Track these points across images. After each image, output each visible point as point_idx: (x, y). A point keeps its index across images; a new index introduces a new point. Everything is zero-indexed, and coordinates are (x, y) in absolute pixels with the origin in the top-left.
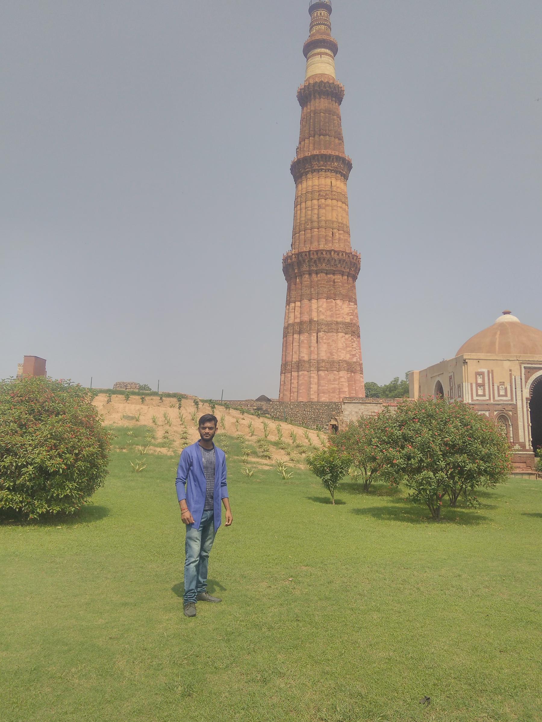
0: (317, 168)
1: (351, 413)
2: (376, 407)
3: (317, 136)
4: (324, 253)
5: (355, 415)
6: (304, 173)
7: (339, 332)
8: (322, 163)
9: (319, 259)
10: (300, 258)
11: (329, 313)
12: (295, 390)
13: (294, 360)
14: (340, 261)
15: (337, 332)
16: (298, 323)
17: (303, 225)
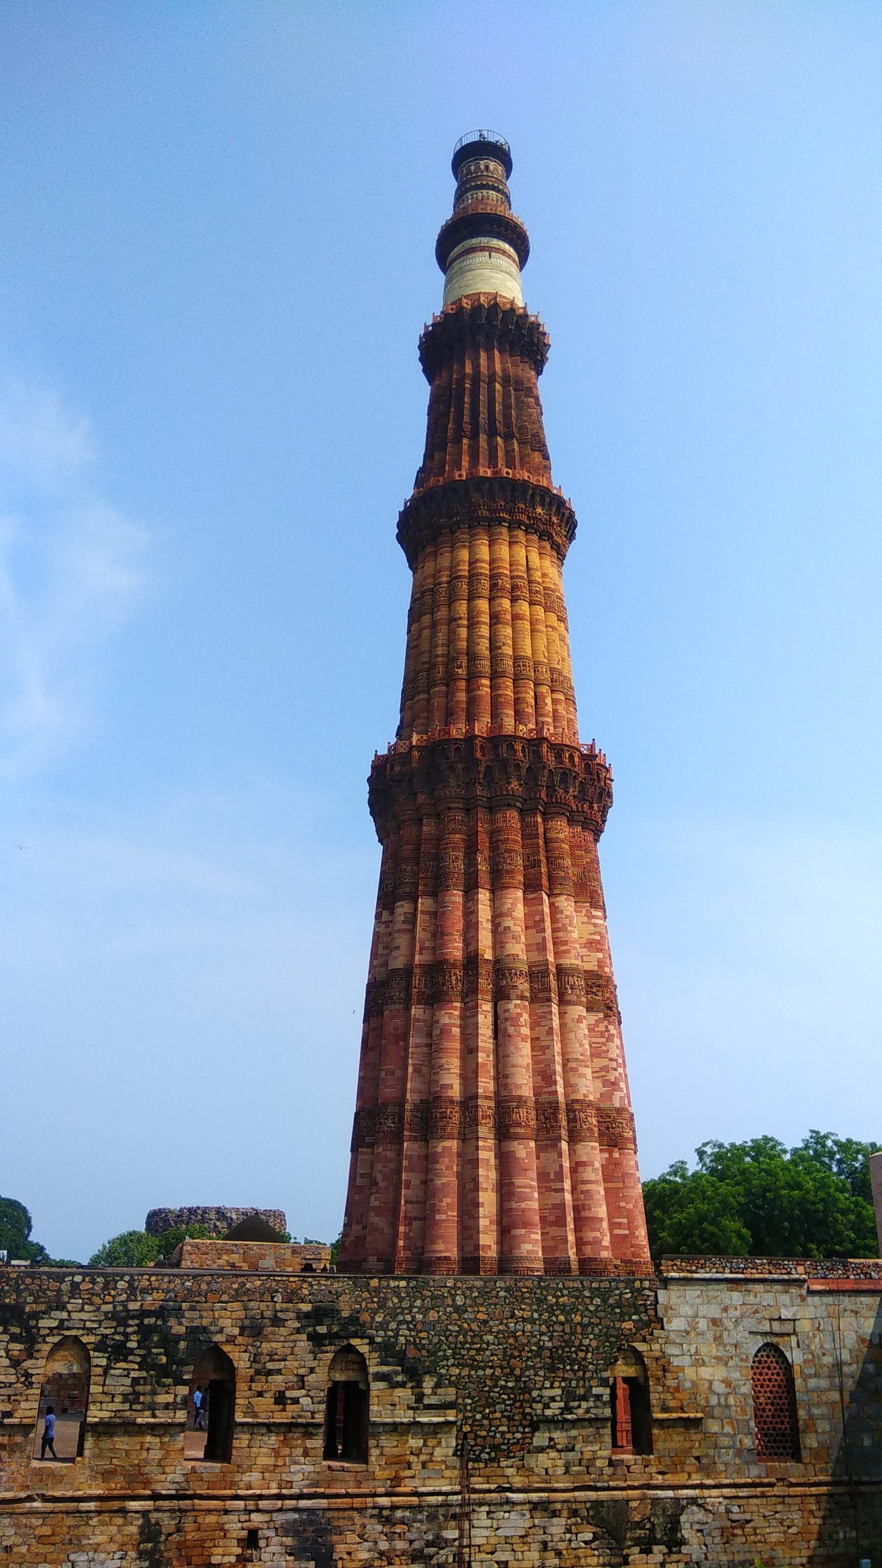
0: (485, 513)
2: (785, 1299)
5: (710, 1335)
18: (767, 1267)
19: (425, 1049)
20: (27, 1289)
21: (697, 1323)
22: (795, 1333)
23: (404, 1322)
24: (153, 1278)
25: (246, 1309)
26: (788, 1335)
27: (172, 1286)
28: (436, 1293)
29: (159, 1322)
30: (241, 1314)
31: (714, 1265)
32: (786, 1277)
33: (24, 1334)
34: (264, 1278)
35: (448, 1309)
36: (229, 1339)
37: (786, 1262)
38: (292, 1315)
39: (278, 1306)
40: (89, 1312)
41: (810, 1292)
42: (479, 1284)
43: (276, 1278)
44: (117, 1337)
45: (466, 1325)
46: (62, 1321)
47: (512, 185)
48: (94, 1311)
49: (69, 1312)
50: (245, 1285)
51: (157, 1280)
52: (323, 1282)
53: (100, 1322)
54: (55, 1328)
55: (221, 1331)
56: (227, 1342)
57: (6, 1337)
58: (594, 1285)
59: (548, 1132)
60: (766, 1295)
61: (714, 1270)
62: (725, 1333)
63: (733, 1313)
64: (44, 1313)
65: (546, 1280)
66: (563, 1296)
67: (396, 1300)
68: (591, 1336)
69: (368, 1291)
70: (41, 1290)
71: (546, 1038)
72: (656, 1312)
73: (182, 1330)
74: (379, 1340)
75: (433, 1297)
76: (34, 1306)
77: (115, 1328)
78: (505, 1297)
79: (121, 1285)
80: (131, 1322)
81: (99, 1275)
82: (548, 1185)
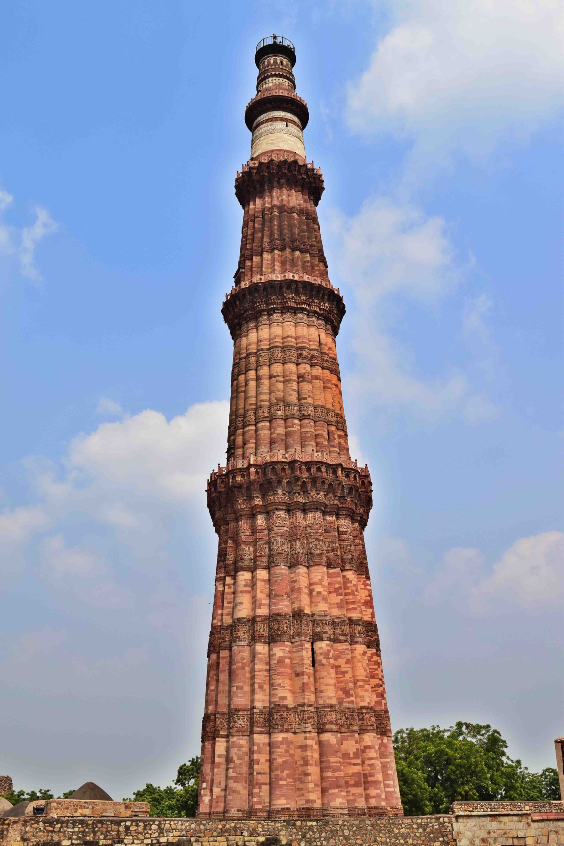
0: (293, 305)
2: (520, 825)
3: (288, 250)
4: (323, 469)
6: (264, 310)
7: (357, 643)
8: (303, 297)
9: (314, 481)
10: (270, 475)
11: (335, 599)
12: (264, 779)
13: (259, 705)
14: (351, 489)
15: (353, 642)
16: (264, 618)
17: (266, 410)
18: (509, 807)
19: (266, 673)
20: (99, 831)
24: (172, 823)
25: (227, 840)
27: (183, 827)
28: (333, 828)
31: (482, 806)
32: (520, 812)
34: (236, 822)
35: (340, 838)
37: (519, 804)
39: (246, 838)
40: (137, 844)
41: (534, 821)
42: (357, 822)
43: (243, 821)
47: (295, 71)
48: (140, 844)
50: (225, 825)
51: (174, 824)
52: (270, 824)
58: (419, 821)
59: (348, 727)
61: (482, 810)
63: (493, 835)
65: (392, 819)
66: (402, 828)
67: (311, 833)
69: (295, 828)
70: (107, 831)
71: (346, 666)
72: (453, 836)
75: (331, 831)
76: (105, 841)
78: (371, 830)
79: (154, 827)
81: (140, 821)
82: (349, 761)
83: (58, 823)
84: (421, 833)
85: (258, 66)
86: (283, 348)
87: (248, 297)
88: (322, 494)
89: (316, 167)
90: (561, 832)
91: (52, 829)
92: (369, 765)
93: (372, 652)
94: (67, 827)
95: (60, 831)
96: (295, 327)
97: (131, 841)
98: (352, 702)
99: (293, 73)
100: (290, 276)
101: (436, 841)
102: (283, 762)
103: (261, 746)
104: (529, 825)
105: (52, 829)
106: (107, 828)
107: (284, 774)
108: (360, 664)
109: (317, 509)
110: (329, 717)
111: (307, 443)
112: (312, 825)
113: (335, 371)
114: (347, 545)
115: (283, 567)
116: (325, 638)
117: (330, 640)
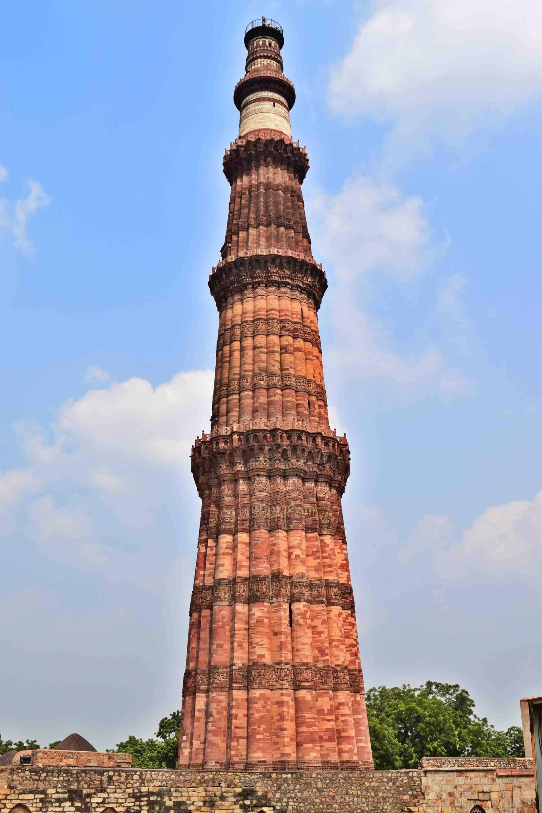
0: (277, 279)
1: (439, 797)
2: (485, 780)
3: (273, 226)
4: (304, 438)
5: (448, 802)
6: (249, 284)
7: (333, 604)
8: (287, 272)
9: (294, 448)
10: (252, 443)
11: (313, 562)
12: (242, 733)
13: (238, 662)
14: (330, 457)
15: (329, 603)
16: (245, 580)
17: (249, 380)
18: (476, 763)
20: (83, 780)
21: (441, 795)
22: (490, 800)
23: (291, 797)
24: (153, 773)
25: (206, 791)
26: (487, 800)
27: (164, 778)
28: (307, 781)
29: (159, 799)
30: (203, 794)
31: (450, 762)
32: (486, 768)
33: (83, 807)
34: (214, 773)
35: (314, 790)
36: (198, 808)
37: (485, 760)
38: (231, 794)
39: (224, 789)
41: (499, 777)
42: (330, 775)
44: (136, 808)
45: (323, 799)
46: (104, 799)
48: (122, 793)
49: (108, 793)
50: (204, 776)
51: (155, 774)
53: (126, 799)
54: (101, 803)
55: (193, 804)
56: (197, 810)
57: (73, 809)
58: (389, 775)
59: (323, 685)
60: (475, 779)
61: (450, 765)
62: (456, 800)
63: (459, 789)
64: (95, 794)
65: (364, 773)
66: (373, 781)
67: (286, 785)
68: (388, 804)
69: (271, 780)
72: (421, 789)
73: (171, 803)
74: (278, 808)
75: (305, 784)
76: (88, 790)
77: (134, 802)
79: (136, 777)
80: (143, 799)
81: (123, 771)
82: (323, 717)
83: (43, 772)
84: (391, 787)
85: (247, 47)
86: (267, 320)
87: (234, 270)
88: (302, 461)
89: (301, 146)
90: (524, 787)
91: (38, 778)
92: (342, 721)
93: (347, 614)
94: (52, 776)
95: (45, 780)
96: (279, 300)
97: (114, 790)
98: (327, 661)
99: (281, 55)
100: (274, 251)
101: (405, 795)
102: (260, 717)
103: (240, 701)
104: (494, 780)
105: (38, 778)
106: (90, 778)
107: (261, 729)
108: (335, 625)
109: (297, 475)
110: (305, 675)
111: (288, 412)
112: (287, 778)
113: (317, 344)
114: (325, 511)
115: (263, 530)
116: (302, 600)
117: (307, 601)
